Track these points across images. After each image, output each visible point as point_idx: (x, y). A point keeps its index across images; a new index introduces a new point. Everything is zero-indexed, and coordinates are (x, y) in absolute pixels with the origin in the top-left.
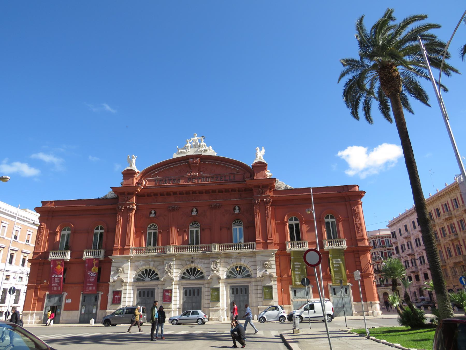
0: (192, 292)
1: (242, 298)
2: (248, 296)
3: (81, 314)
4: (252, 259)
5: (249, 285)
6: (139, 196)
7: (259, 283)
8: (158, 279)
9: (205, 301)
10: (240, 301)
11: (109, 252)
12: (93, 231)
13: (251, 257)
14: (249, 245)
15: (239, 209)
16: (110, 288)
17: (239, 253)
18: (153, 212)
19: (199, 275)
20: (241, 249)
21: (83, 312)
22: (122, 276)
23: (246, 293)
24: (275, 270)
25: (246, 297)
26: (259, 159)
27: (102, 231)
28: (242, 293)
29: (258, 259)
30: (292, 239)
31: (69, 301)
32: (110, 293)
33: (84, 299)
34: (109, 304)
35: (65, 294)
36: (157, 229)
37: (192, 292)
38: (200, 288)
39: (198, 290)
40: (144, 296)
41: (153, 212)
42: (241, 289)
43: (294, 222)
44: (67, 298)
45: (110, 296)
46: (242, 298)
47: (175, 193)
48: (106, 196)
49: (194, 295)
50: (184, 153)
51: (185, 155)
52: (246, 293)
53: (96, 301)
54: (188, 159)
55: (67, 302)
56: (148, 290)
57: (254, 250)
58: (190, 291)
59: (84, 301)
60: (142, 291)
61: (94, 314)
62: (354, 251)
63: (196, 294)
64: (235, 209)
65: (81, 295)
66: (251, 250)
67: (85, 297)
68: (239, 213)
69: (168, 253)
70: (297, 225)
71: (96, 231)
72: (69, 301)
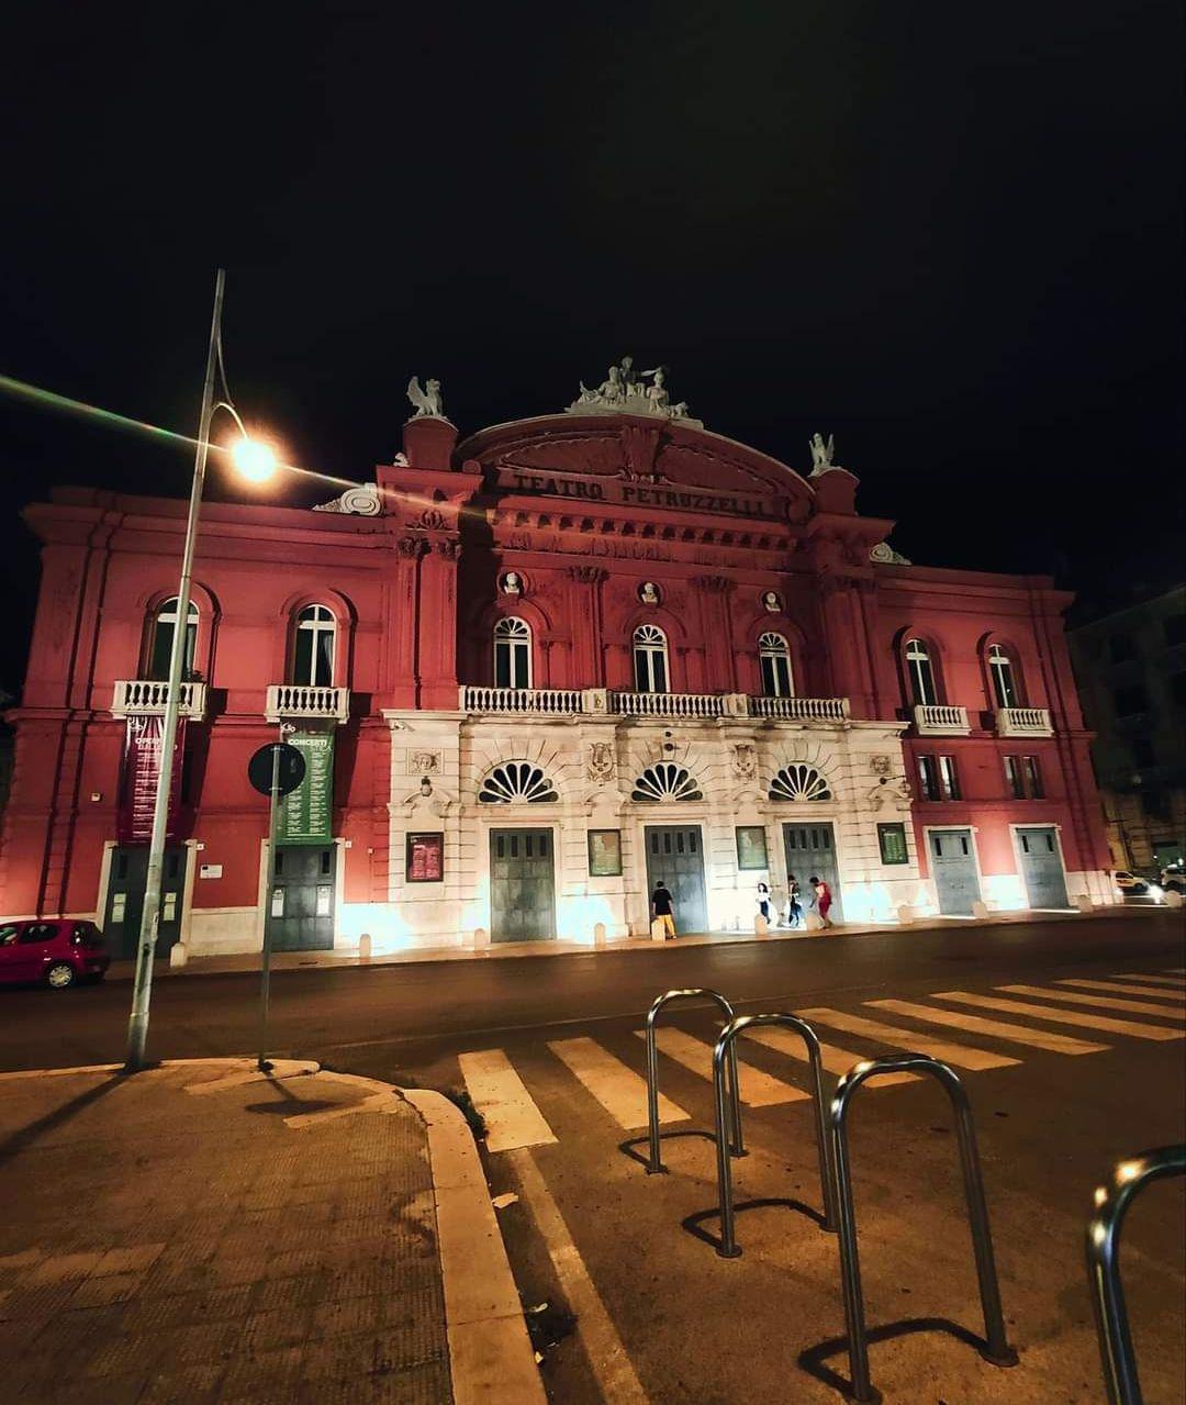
0: (674, 841)
2: (833, 853)
3: (270, 919)
5: (835, 821)
10: (813, 868)
16: (394, 825)
23: (827, 846)
25: (828, 857)
31: (215, 872)
37: (674, 841)
38: (698, 828)
39: (692, 836)
42: (814, 832)
44: (203, 861)
55: (204, 874)
56: (530, 834)
58: (667, 836)
63: (687, 847)
72: (215, 872)
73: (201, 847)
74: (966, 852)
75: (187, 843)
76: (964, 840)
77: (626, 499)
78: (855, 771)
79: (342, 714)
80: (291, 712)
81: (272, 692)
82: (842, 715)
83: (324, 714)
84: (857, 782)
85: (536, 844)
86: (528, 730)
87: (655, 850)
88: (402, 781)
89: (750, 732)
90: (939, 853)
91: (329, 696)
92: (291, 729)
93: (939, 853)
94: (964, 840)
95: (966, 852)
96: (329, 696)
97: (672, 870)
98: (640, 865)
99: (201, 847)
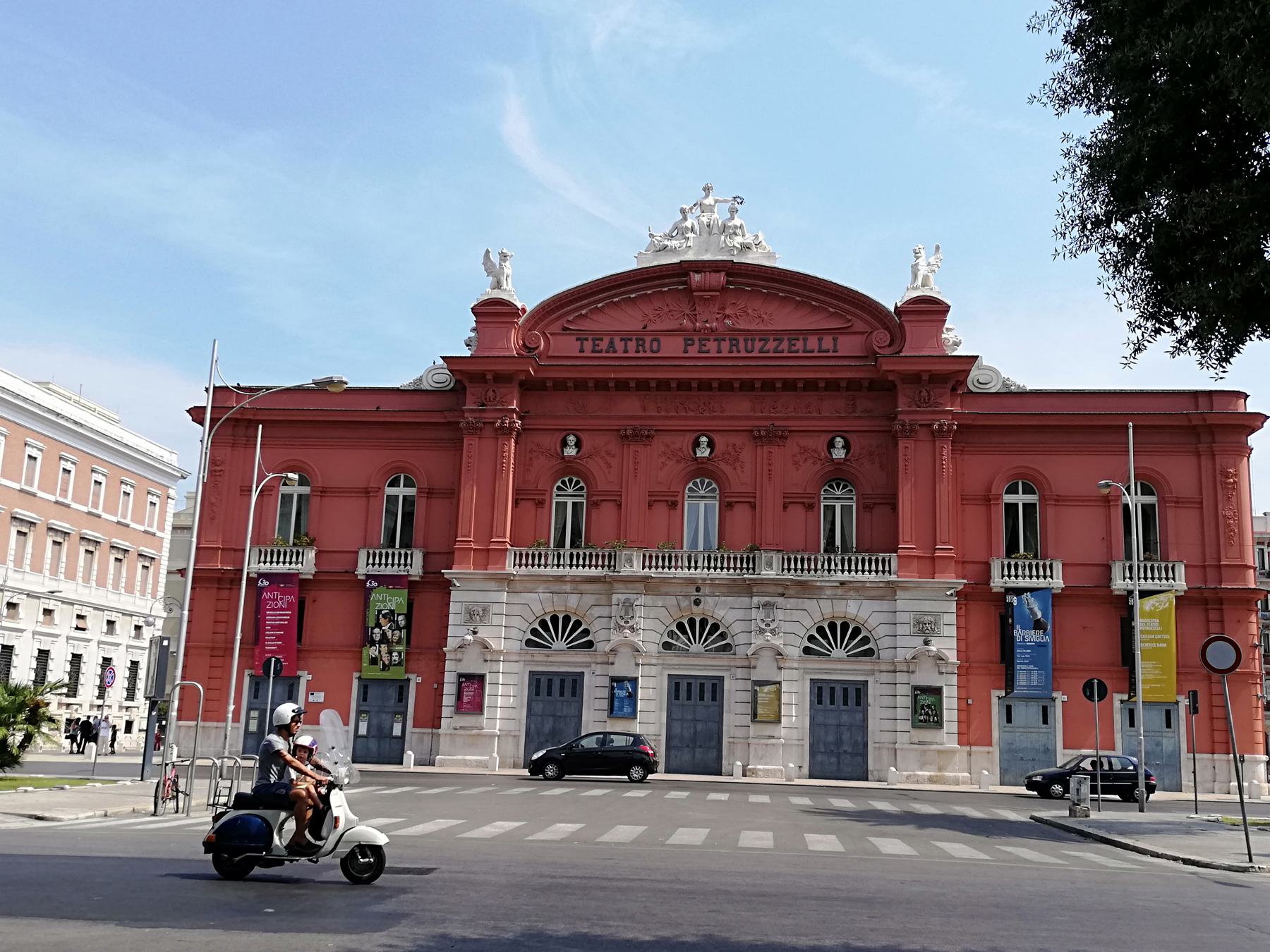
0: (696, 690)
1: (845, 718)
3: (356, 736)
4: (885, 605)
5: (871, 680)
6: (529, 387)
7: (901, 678)
8: (590, 644)
9: (734, 717)
11: (442, 554)
12: (380, 490)
13: (881, 598)
14: (877, 561)
15: (847, 446)
17: (842, 583)
18: (571, 439)
19: (713, 642)
20: (849, 571)
21: (363, 730)
22: (483, 633)
23: (858, 704)
24: (953, 643)
26: (923, 285)
27: (412, 491)
28: (845, 703)
29: (900, 605)
30: (1012, 549)
32: (449, 678)
33: (365, 693)
34: (445, 712)
35: (305, 677)
36: (584, 492)
37: (696, 690)
38: (721, 679)
40: (549, 694)
41: (571, 439)
42: (845, 690)
43: (1020, 499)
44: (311, 689)
45: (449, 689)
46: (845, 718)
47: (643, 385)
48: (420, 379)
49: (702, 698)
50: (674, 250)
51: (676, 260)
52: (858, 704)
53: (400, 700)
54: (687, 274)
55: (311, 699)
57: (893, 578)
58: (689, 685)
59: (365, 699)
60: (544, 680)
61: (396, 737)
62: (1205, 601)
63: (708, 695)
64: (831, 445)
65: (355, 683)
66: (881, 577)
67: (366, 687)
68: (845, 460)
69: (625, 571)
70: (1028, 507)
71: (390, 491)
73: (310, 677)
74: (1045, 722)
75: (300, 673)
76: (1045, 709)
77: (686, 352)
78: (901, 630)
79: (416, 569)
80: (376, 570)
81: (362, 555)
82: (890, 572)
83: (402, 571)
84: (900, 642)
85: (568, 685)
86: (568, 587)
87: (677, 698)
88: (457, 632)
89: (780, 590)
90: (1009, 720)
91: (406, 555)
92: (374, 584)
93: (1009, 720)
94: (1045, 709)
95: (1045, 722)
96: (406, 555)
97: (690, 717)
98: (661, 710)
99: (310, 677)
